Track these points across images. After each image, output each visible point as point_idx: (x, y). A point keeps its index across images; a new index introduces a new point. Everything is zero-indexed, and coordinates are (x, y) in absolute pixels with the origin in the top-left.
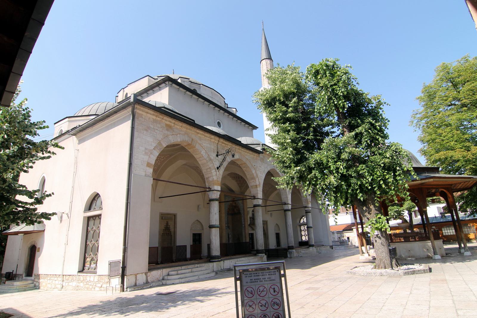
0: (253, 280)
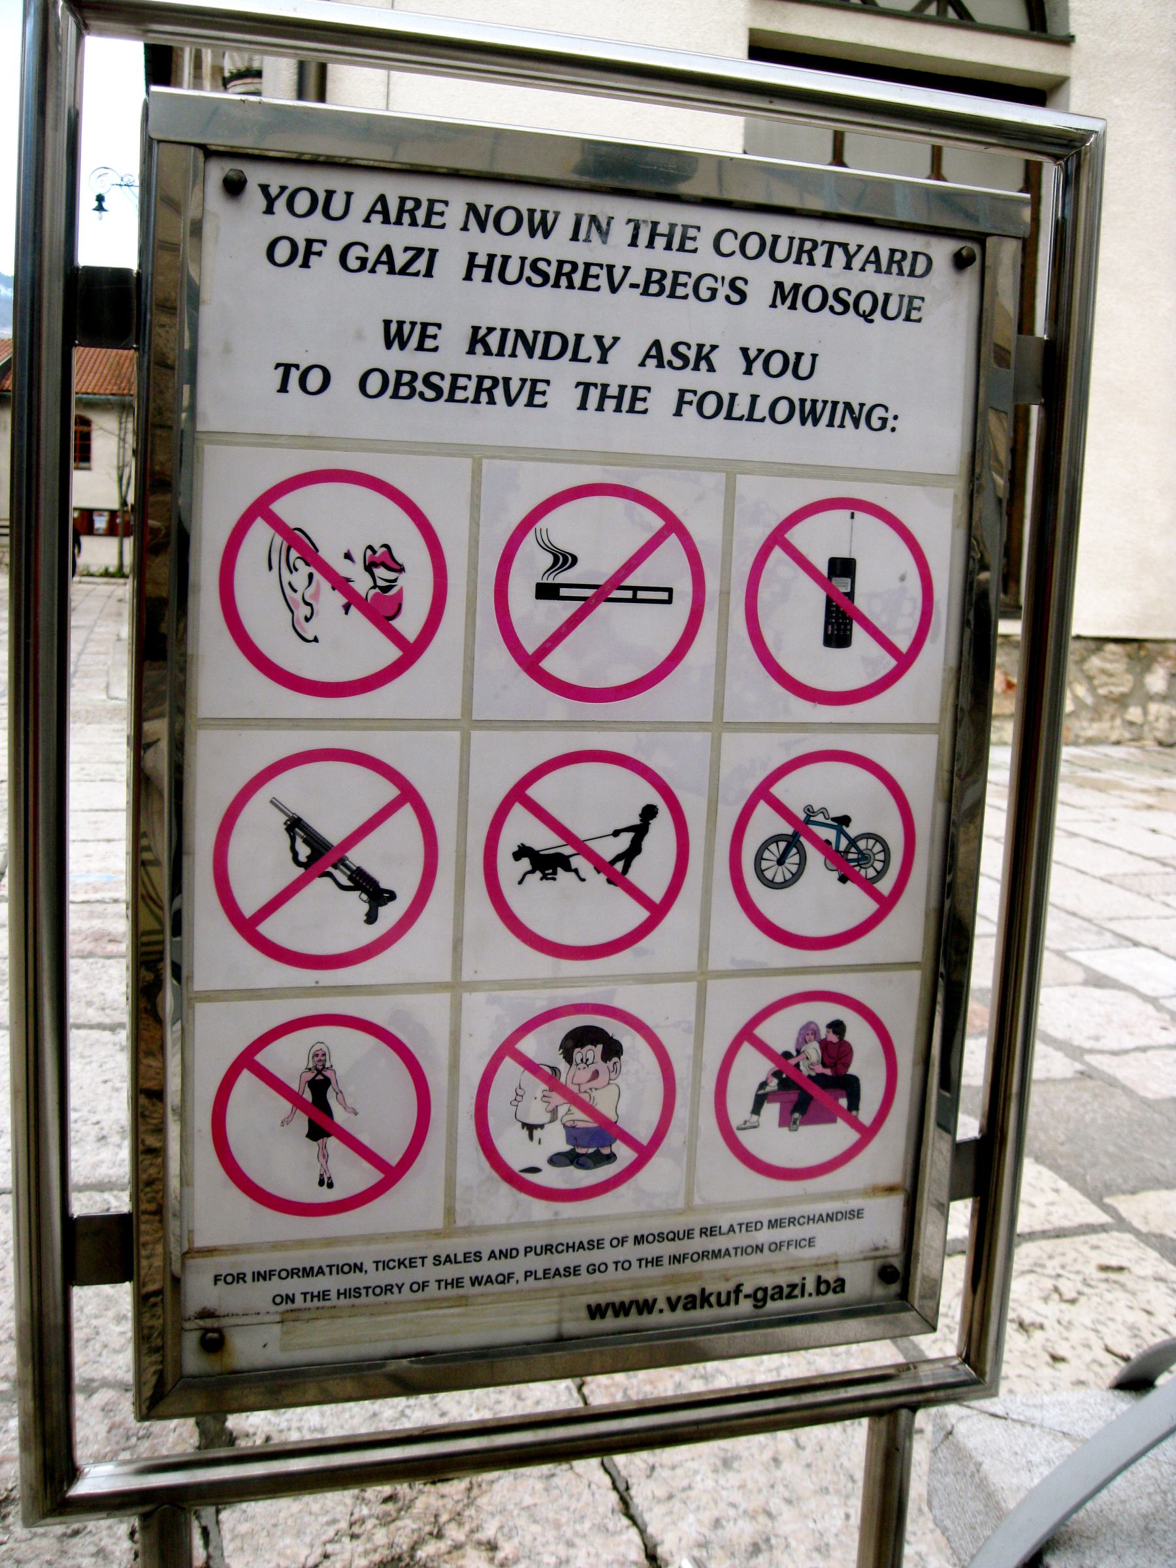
0: (451, 356)
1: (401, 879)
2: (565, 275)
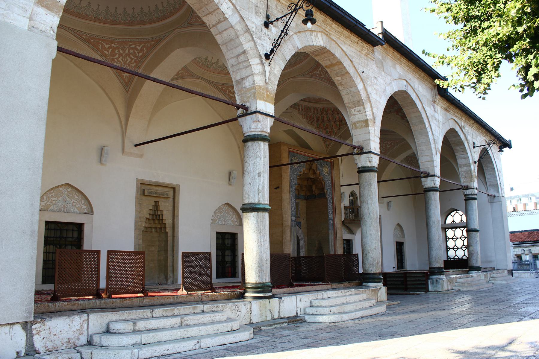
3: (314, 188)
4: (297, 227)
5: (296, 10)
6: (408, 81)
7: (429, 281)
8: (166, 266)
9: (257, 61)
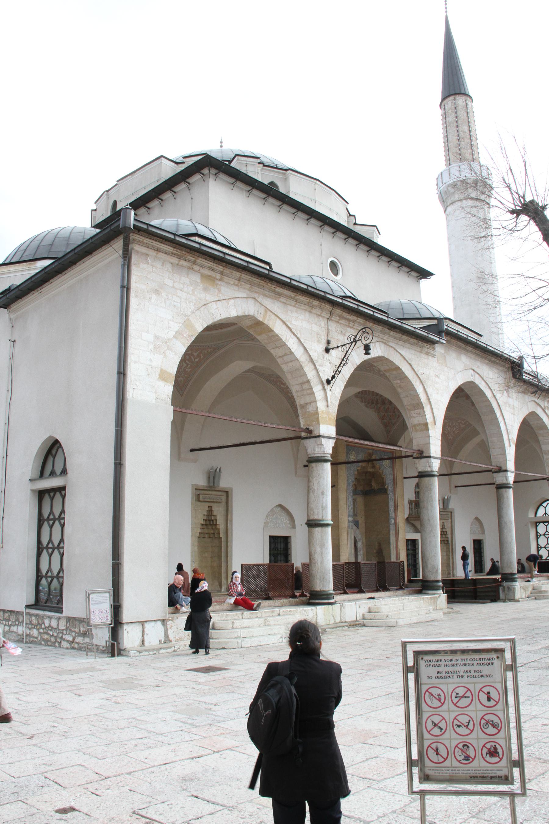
0: (444, 674)
1: (444, 727)
2: (454, 665)
3: (373, 484)
4: (355, 527)
5: (355, 341)
6: (476, 369)
7: (501, 588)
8: (220, 573)
9: (320, 387)
